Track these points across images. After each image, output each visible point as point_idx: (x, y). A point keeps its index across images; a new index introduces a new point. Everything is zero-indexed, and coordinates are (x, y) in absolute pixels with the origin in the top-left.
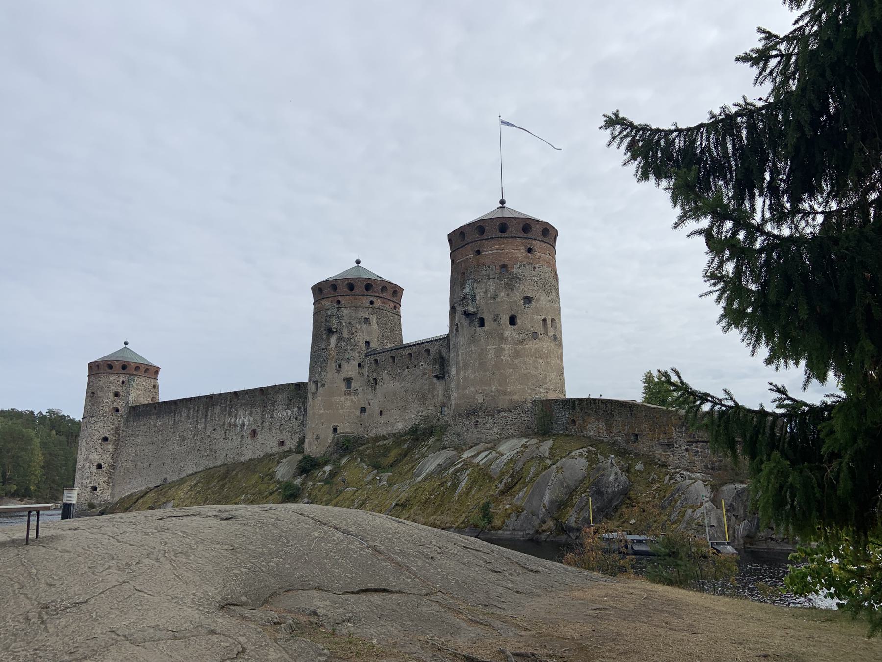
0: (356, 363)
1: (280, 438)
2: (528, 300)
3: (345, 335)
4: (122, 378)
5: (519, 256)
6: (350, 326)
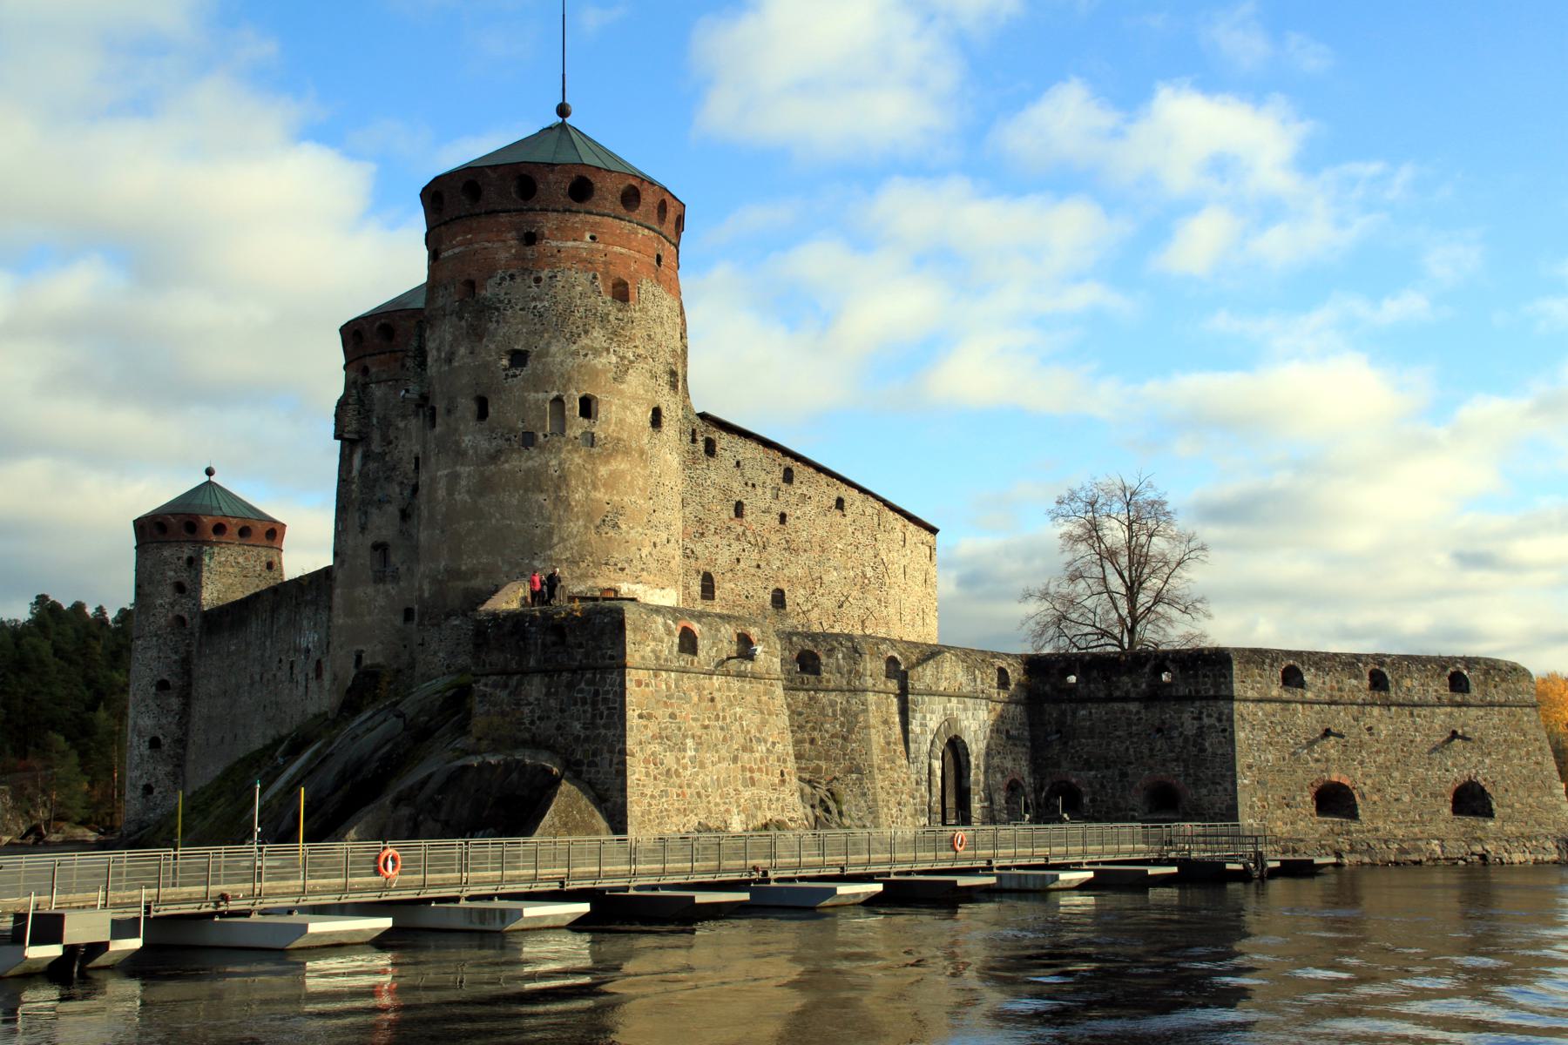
0: (393, 510)
2: (519, 358)
3: (376, 447)
4: (187, 552)
5: (503, 256)
6: (386, 423)
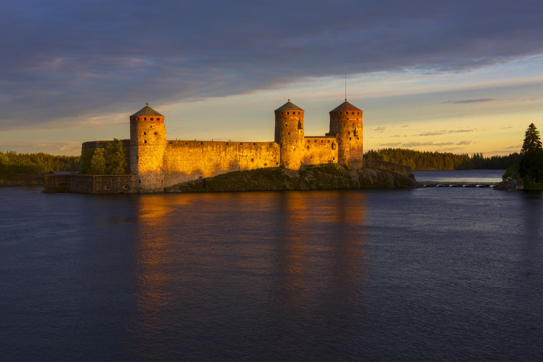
1: (264, 162)
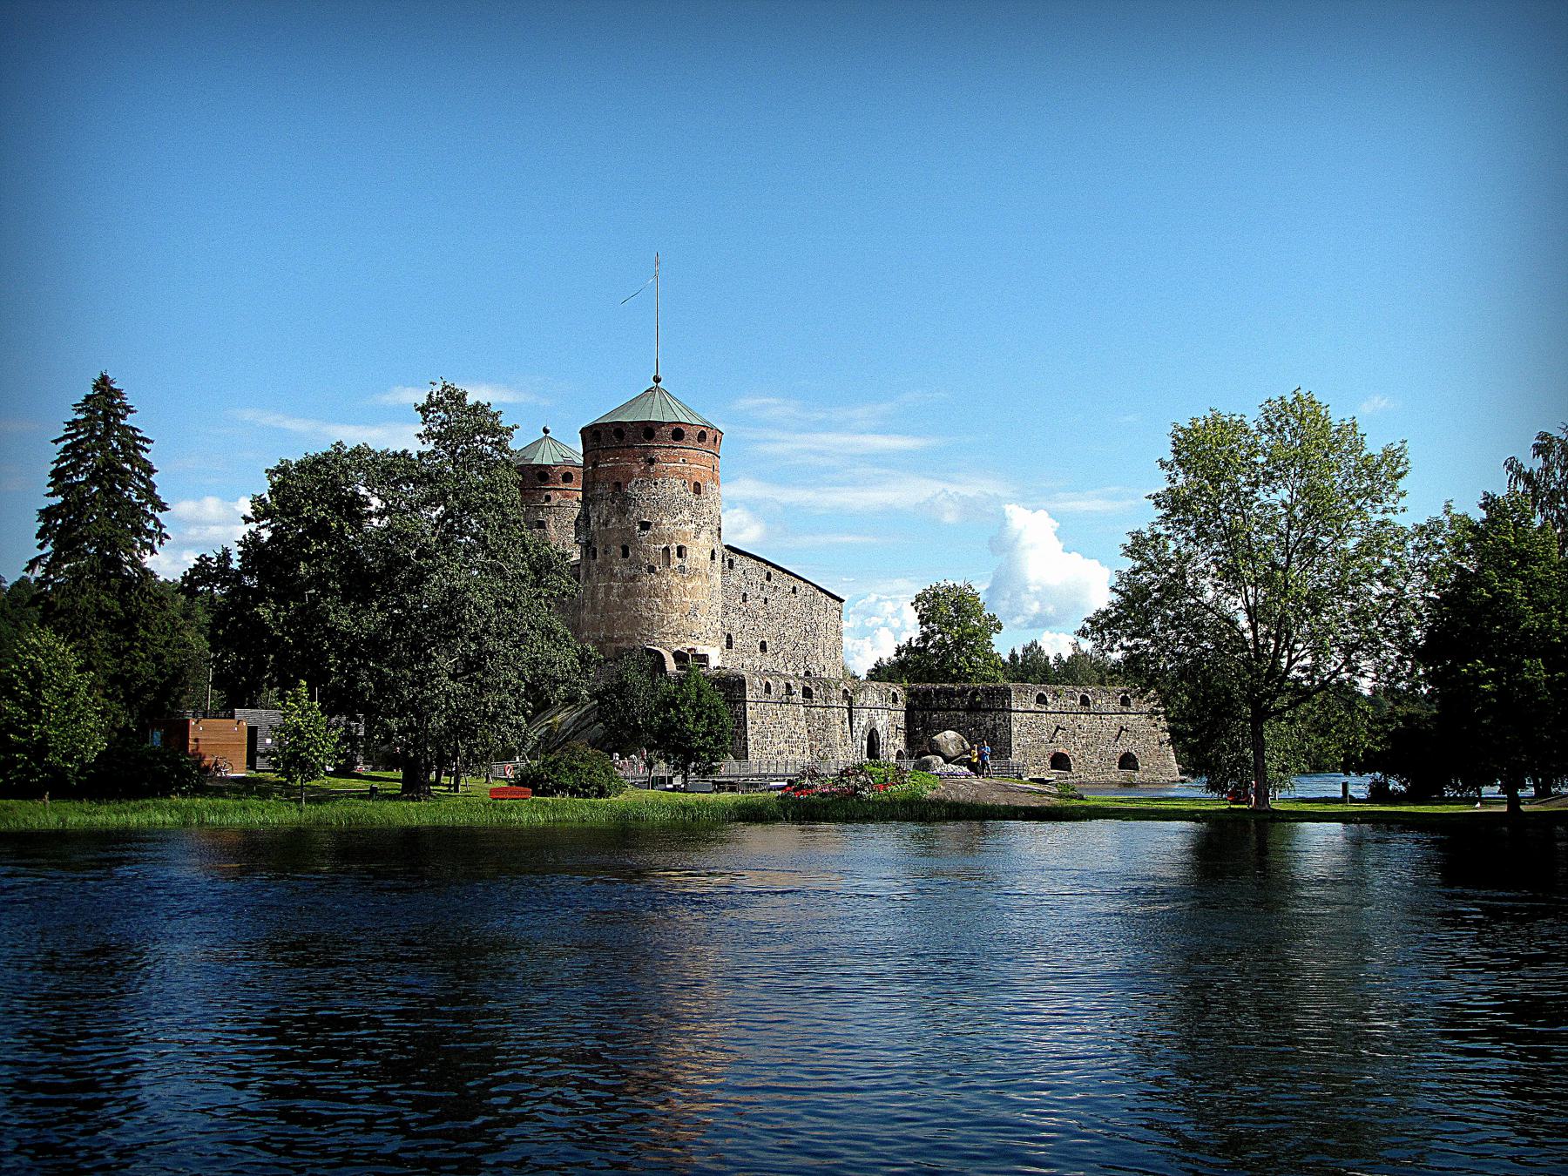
2: (645, 526)
